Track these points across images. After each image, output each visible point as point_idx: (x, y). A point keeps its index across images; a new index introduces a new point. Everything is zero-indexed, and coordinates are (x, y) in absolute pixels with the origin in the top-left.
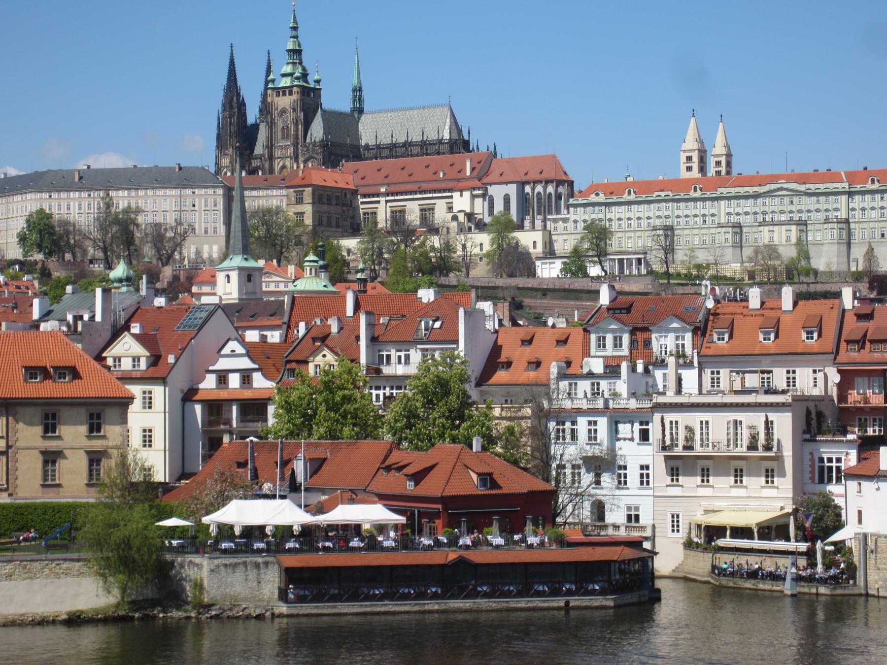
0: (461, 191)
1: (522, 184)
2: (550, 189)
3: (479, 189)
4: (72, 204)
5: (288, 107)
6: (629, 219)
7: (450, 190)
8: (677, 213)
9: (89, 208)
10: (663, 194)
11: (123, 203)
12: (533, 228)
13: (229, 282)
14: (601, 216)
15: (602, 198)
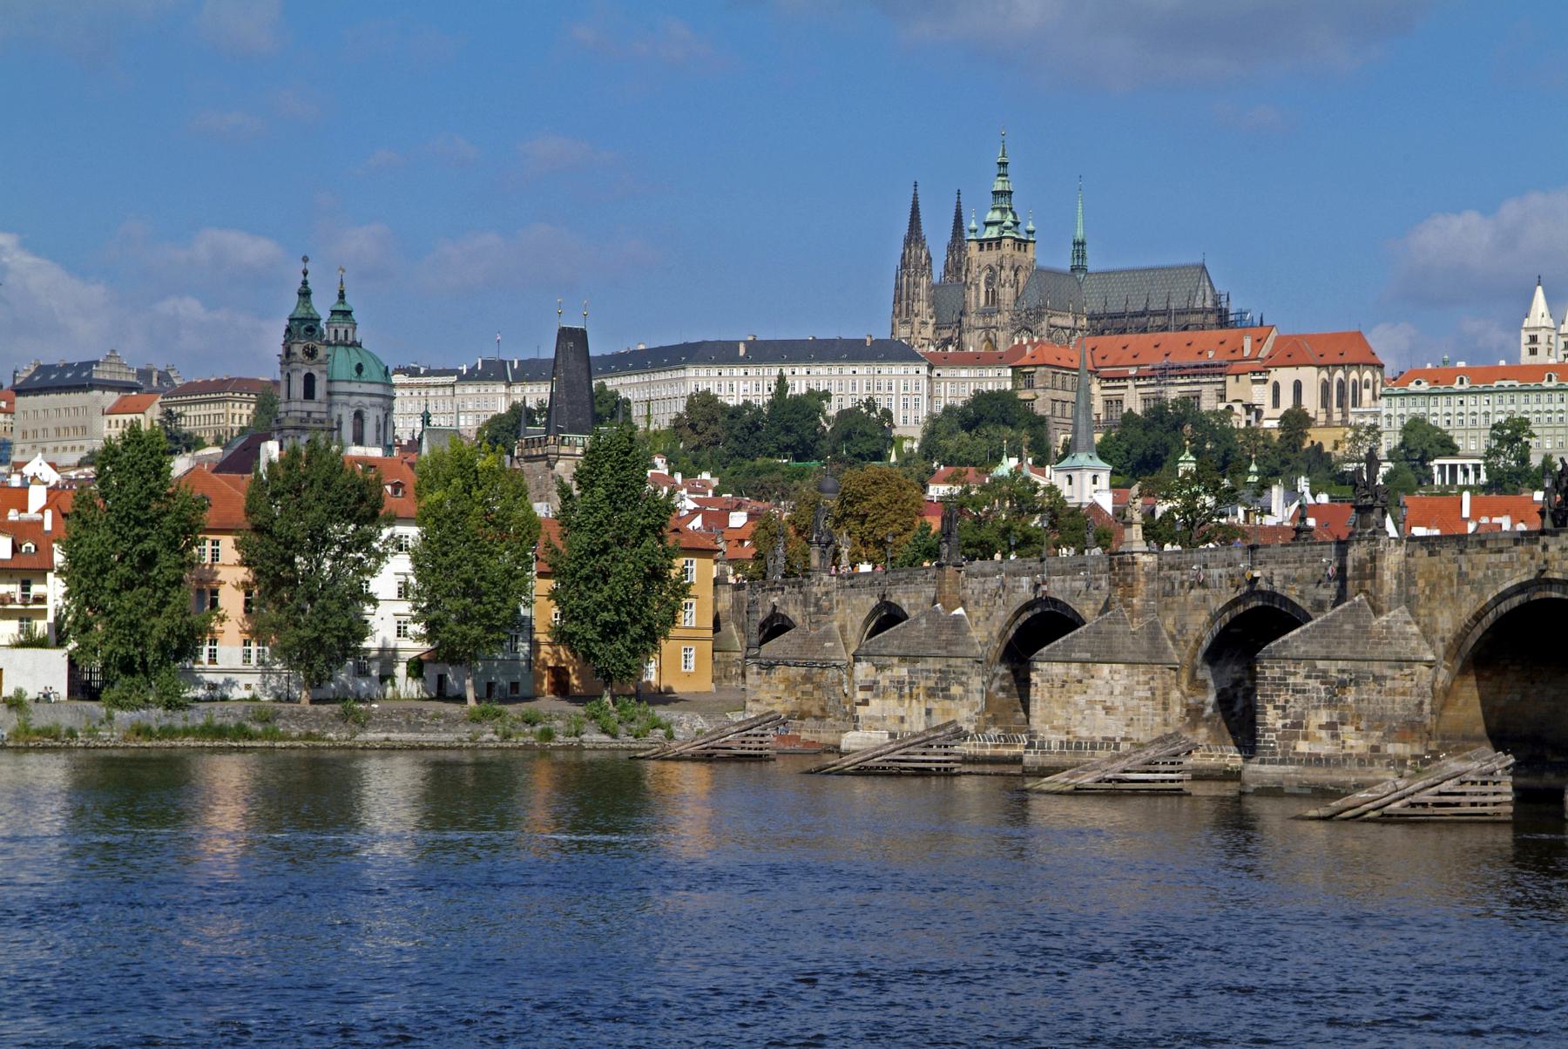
0: (1237, 375)
1: (1319, 367)
2: (1354, 375)
3: (1260, 373)
4: (735, 384)
5: (994, 265)
6: (1461, 414)
7: (1221, 374)
8: (1528, 407)
9: (758, 389)
10: (1506, 383)
11: (800, 384)
12: (1328, 424)
13: (1070, 483)
14: (1423, 410)
15: (1425, 387)
